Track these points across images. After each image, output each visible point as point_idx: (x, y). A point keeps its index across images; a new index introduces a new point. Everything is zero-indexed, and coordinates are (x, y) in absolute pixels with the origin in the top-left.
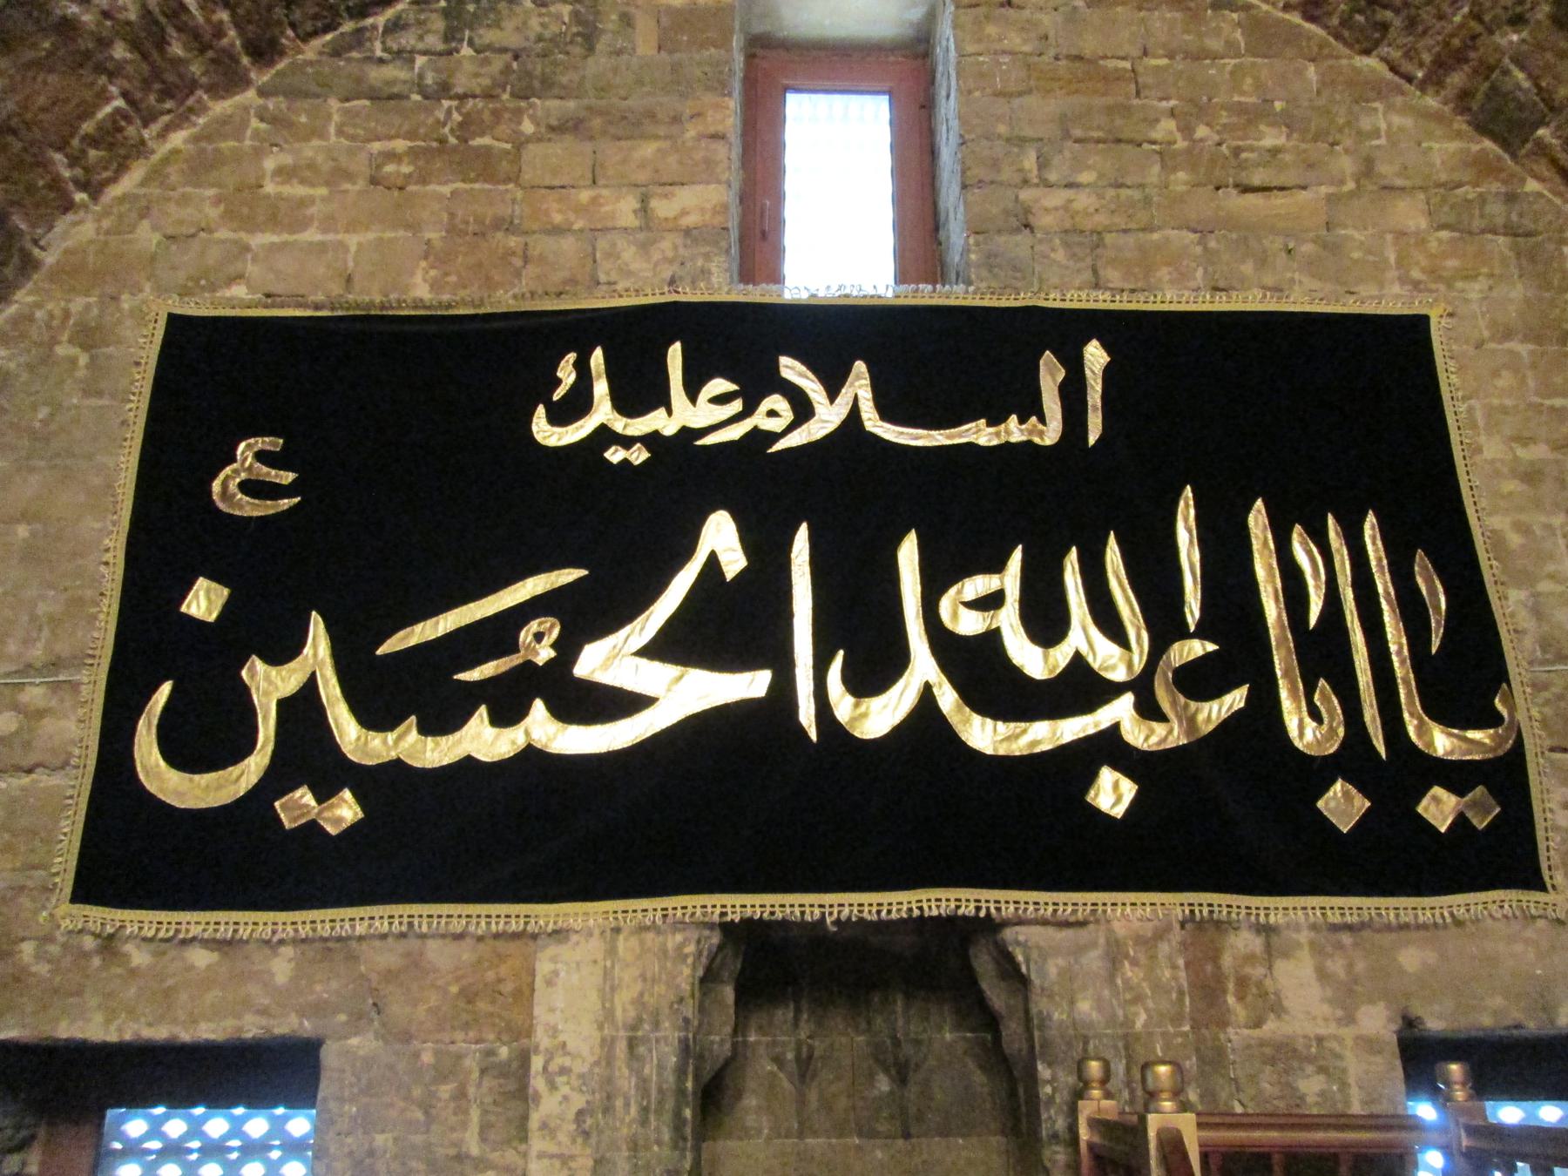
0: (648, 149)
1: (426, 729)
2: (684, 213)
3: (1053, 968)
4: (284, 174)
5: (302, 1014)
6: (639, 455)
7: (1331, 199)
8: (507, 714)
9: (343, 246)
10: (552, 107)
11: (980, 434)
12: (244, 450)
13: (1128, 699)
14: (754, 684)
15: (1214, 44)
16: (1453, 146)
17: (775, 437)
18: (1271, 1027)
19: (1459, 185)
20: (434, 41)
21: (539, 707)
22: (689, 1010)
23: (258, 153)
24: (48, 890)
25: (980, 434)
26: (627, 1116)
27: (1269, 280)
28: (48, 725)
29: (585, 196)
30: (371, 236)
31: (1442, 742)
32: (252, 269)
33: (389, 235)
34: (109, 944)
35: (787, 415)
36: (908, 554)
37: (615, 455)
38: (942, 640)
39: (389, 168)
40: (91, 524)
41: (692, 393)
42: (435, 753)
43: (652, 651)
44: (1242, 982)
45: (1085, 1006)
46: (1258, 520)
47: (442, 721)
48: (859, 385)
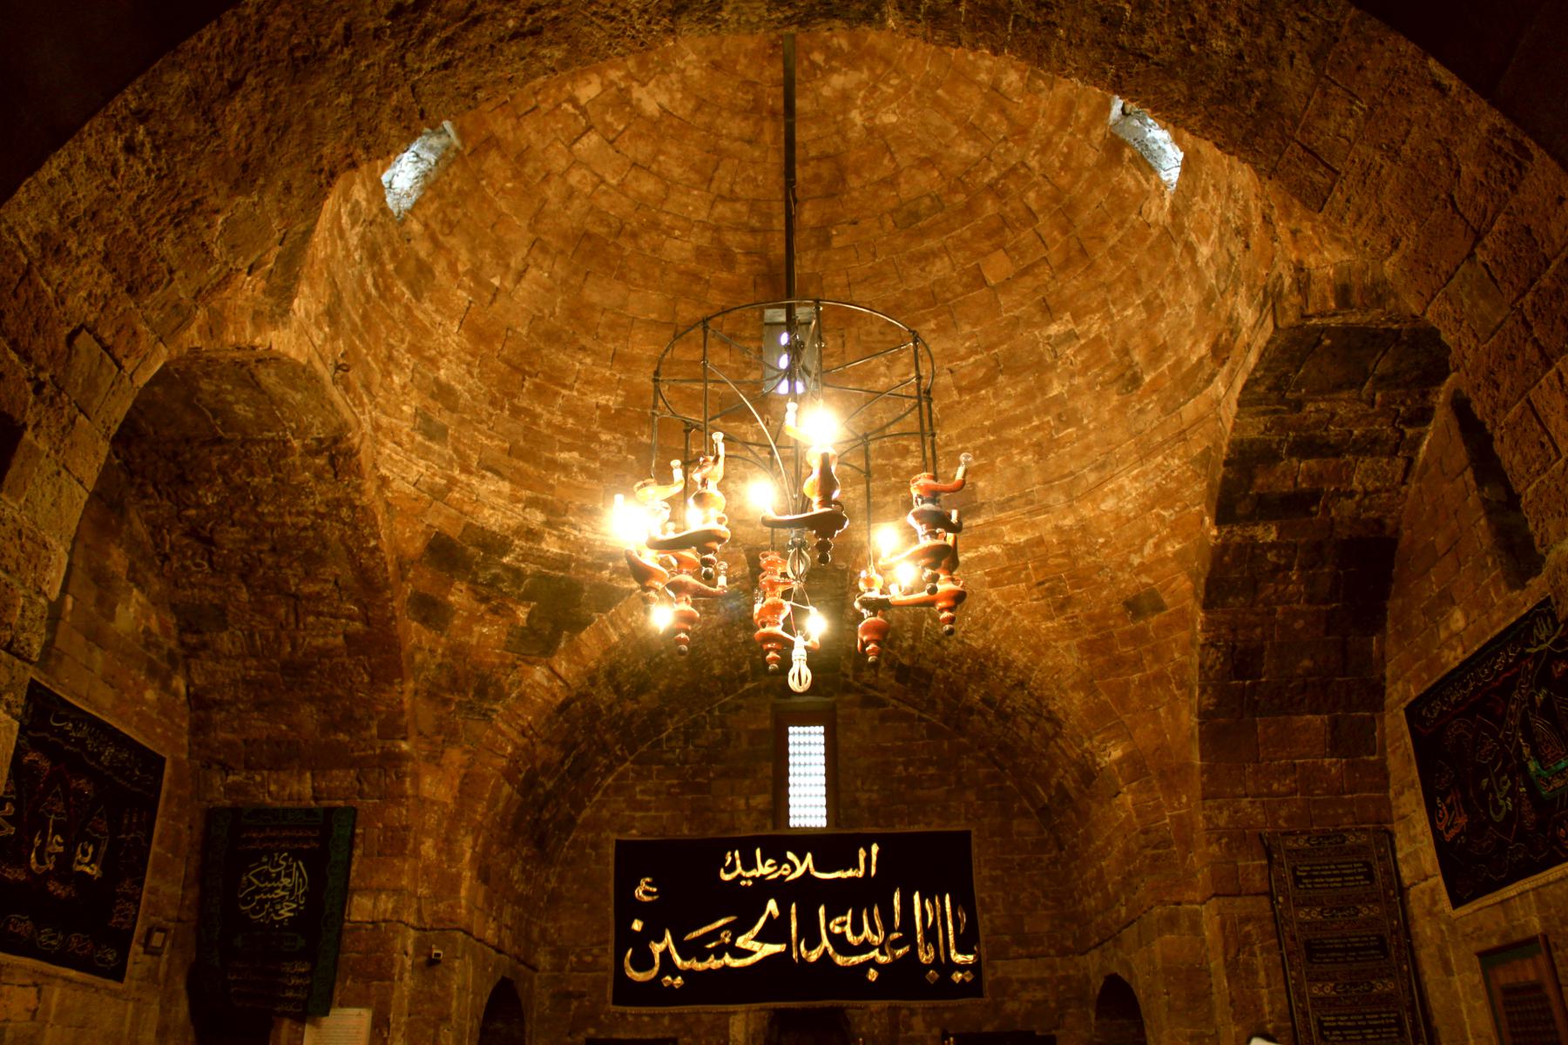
0: (747, 782)
3: (856, 1019)
4: (643, 792)
6: (750, 883)
8: (719, 956)
9: (661, 817)
10: (717, 767)
12: (642, 882)
13: (877, 950)
14: (778, 948)
17: (786, 877)
18: (910, 1033)
20: (681, 743)
24: (606, 1002)
31: (958, 958)
32: (637, 824)
36: (822, 910)
37: (743, 883)
41: (763, 862)
42: (700, 966)
43: (755, 939)
46: (917, 897)
47: (702, 959)
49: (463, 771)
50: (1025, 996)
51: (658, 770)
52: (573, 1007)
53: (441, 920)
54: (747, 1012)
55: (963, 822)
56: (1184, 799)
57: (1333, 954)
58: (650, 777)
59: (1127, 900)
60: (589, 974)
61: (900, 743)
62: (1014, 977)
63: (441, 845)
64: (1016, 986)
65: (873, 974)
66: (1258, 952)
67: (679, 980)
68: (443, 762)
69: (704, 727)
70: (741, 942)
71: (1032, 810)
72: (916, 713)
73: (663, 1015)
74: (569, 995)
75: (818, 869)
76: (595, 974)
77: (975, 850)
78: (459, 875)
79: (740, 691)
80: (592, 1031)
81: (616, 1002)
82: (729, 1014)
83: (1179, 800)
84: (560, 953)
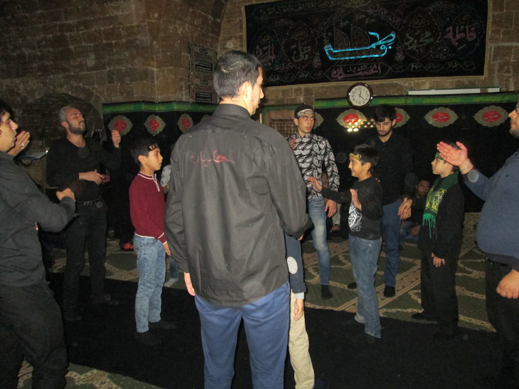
56: (156, 15)
57: (201, 99)
66: (184, 95)
83: (153, 14)
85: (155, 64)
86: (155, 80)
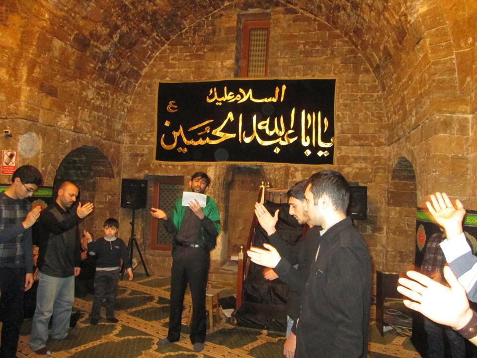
0: (222, 54)
1: (195, 140)
2: (228, 65)
4: (173, 59)
5: (182, 173)
6: (220, 104)
7: (326, 58)
8: (204, 139)
9: (181, 71)
11: (266, 100)
14: (233, 136)
15: (312, 29)
16: (347, 48)
17: (238, 101)
19: (347, 55)
20: (192, 35)
21: (208, 138)
22: (225, 174)
23: (168, 56)
24: (153, 159)
25: (266, 100)
26: (218, 186)
27: (312, 74)
28: (151, 139)
29: (214, 62)
30: (184, 70)
31: (322, 144)
32: (169, 75)
33: (187, 69)
34: (160, 165)
35: (240, 98)
36: (255, 118)
37: (217, 104)
38: (258, 130)
39: (187, 58)
40: (153, 113)
41: (228, 94)
42: (196, 144)
43: (221, 131)
44: (291, 174)
45: (271, 176)
46: (303, 113)
47: (196, 140)
48: (250, 92)
49: (22, 29)
50: (357, 165)
51: (180, 48)
52: (139, 160)
53: (11, 114)
54: (216, 166)
55: (332, 75)
56: (470, 40)
58: (176, 52)
59: (417, 113)
60: (146, 146)
61: (302, 33)
62: (351, 155)
63: (11, 72)
64: (352, 160)
65: (277, 150)
67: (186, 150)
68: (8, 23)
69: (203, 26)
70: (217, 132)
71: (371, 69)
72: (313, 17)
73: (178, 166)
74: (137, 155)
75: (254, 97)
76: (148, 146)
77: (337, 90)
78: (20, 89)
79: (222, 7)
80: (147, 172)
81: (158, 158)
82: (207, 166)
84: (133, 136)
85: (468, 109)
86: (470, 130)
